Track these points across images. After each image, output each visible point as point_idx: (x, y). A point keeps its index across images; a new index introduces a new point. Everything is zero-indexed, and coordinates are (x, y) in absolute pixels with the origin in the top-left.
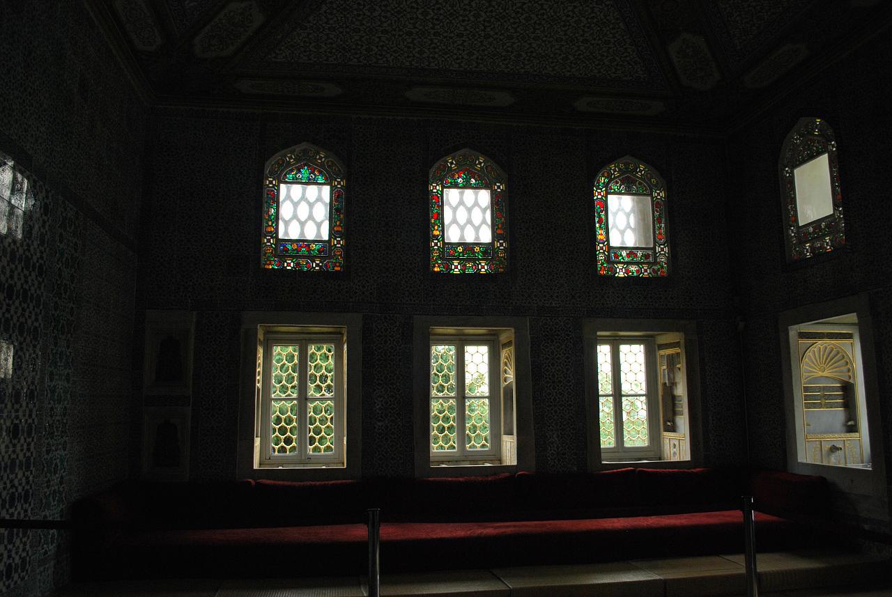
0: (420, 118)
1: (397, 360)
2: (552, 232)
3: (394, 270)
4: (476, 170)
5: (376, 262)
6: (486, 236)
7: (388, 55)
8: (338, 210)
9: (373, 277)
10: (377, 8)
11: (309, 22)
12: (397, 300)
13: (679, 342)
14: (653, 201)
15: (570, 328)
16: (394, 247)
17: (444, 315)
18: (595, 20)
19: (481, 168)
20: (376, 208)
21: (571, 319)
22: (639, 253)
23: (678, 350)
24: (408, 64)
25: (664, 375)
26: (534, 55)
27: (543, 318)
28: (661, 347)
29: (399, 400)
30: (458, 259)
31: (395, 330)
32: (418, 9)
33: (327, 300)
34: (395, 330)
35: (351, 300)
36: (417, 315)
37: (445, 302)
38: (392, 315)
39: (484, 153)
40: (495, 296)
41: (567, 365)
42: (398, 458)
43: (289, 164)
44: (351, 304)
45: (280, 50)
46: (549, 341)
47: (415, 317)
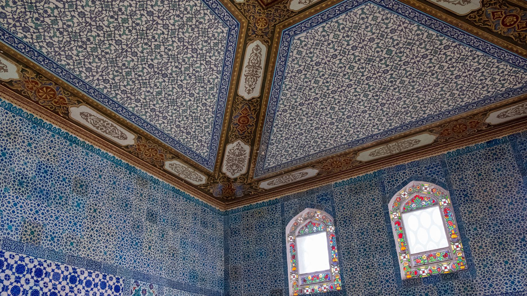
0: (376, 171)
2: (499, 227)
3: (375, 283)
4: (424, 194)
5: (361, 279)
6: (444, 243)
7: (329, 141)
8: (333, 247)
10: (303, 117)
11: (272, 140)
16: (372, 266)
18: (454, 60)
19: (428, 192)
20: (356, 241)
24: (344, 141)
26: (426, 102)
32: (326, 108)
39: (426, 180)
40: (460, 290)
43: (300, 224)
45: (268, 160)
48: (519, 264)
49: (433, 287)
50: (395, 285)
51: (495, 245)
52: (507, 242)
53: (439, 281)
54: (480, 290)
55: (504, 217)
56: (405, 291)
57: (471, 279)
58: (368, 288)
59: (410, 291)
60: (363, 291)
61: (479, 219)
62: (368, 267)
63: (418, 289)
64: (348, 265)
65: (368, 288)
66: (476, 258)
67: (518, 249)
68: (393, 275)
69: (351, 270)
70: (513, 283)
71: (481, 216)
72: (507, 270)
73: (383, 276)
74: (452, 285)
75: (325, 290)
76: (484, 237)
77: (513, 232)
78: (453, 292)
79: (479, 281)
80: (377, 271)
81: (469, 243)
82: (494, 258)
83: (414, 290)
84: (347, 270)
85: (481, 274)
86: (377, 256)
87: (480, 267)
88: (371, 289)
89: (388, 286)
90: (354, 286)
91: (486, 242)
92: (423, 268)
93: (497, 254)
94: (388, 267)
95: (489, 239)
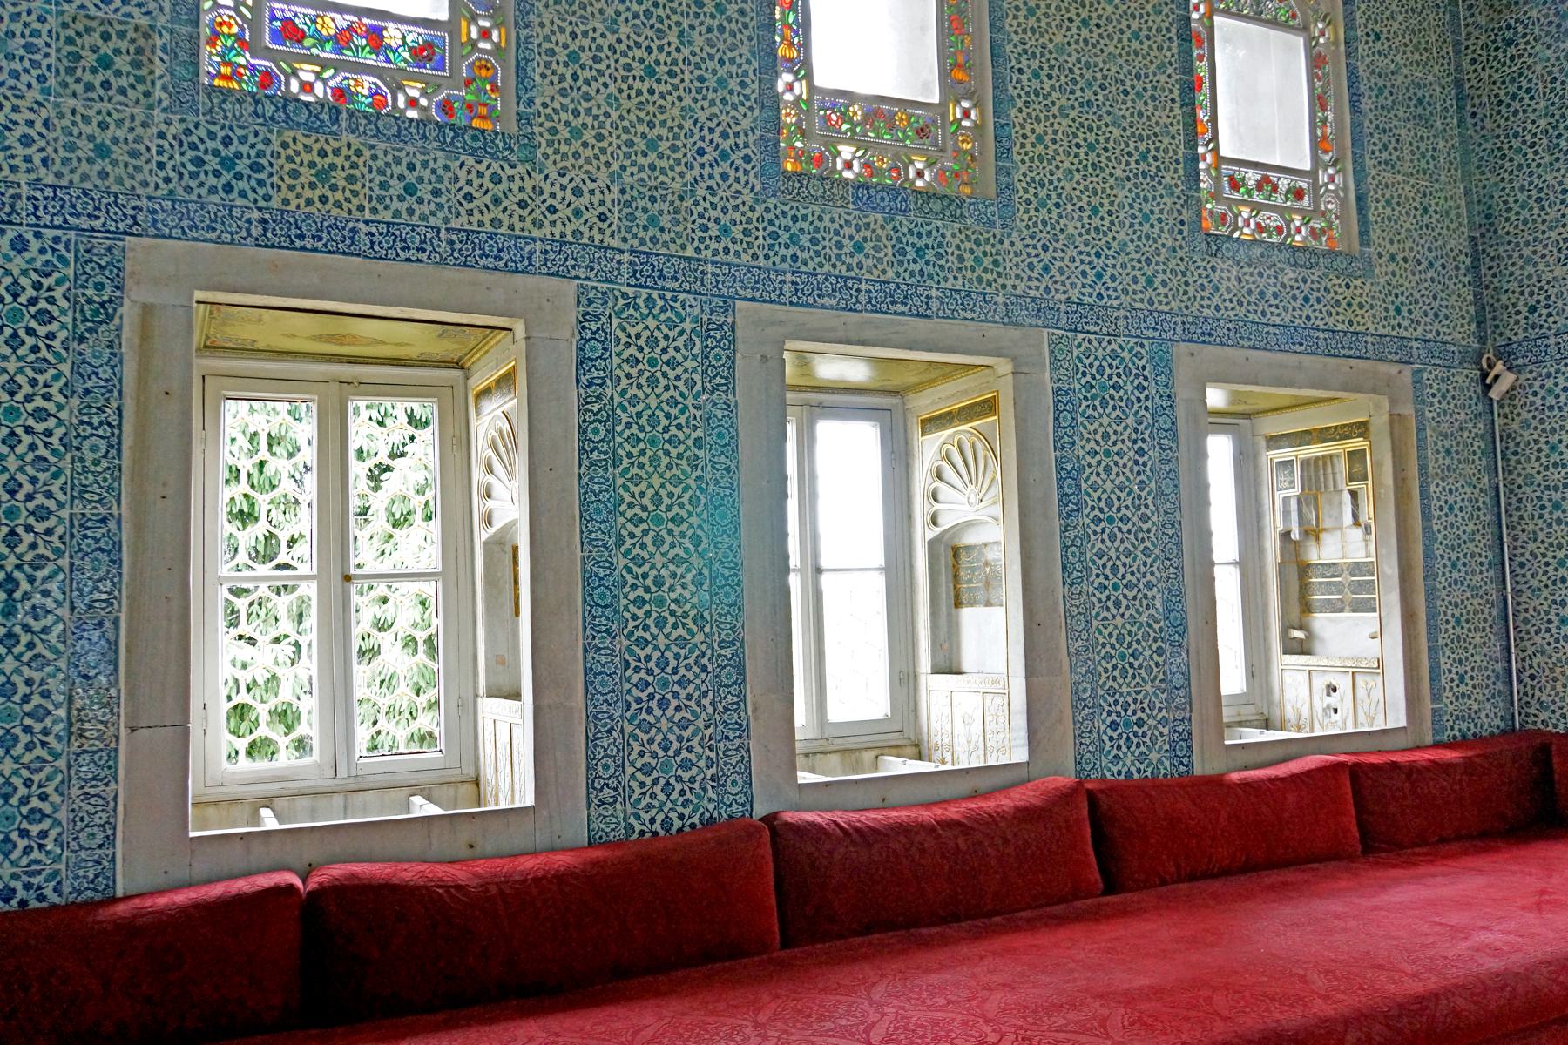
1: (690, 442)
3: (674, 149)
5: (615, 115)
9: (607, 164)
12: (684, 247)
13: (1364, 424)
14: (1309, 48)
15: (1144, 368)
17: (823, 307)
21: (1145, 342)
22: (1284, 182)
23: (1357, 444)
25: (1286, 513)
27: (1081, 336)
28: (1275, 441)
29: (700, 573)
30: (850, 141)
31: (680, 343)
33: (454, 224)
34: (680, 343)
35: (536, 233)
36: (745, 299)
37: (827, 268)
38: (669, 295)
40: (961, 259)
41: (1139, 473)
42: (702, 764)
44: (538, 246)
46: (1097, 403)
47: (739, 304)
48: (1122, 224)
49: (883, 227)
50: (752, 180)
51: (1078, 146)
52: (1106, 150)
53: (904, 212)
54: (1017, 276)
55: (1114, 70)
56: (784, 214)
57: (998, 232)
58: (641, 160)
59: (805, 218)
60: (615, 167)
61: (1051, 46)
62: (650, 72)
63: (832, 220)
64: (562, 30)
65: (641, 160)
66: (1023, 169)
67: (1128, 179)
68: (752, 139)
69: (574, 57)
70: (1099, 276)
71: (1058, 39)
72: (1093, 233)
73: (711, 130)
74: (943, 236)
75: (412, 114)
76: (1055, 110)
77: (1125, 124)
78: (942, 262)
79: (1019, 245)
80: (687, 101)
81: (1014, 112)
82: (1068, 186)
83: (820, 219)
84: (552, 53)
85: (1028, 227)
86: (699, 41)
87: (1028, 202)
88: (652, 167)
89: (724, 176)
90: (576, 133)
91: (1056, 127)
92: (846, 151)
93: (1077, 177)
94: (735, 99)
95: (1065, 123)
